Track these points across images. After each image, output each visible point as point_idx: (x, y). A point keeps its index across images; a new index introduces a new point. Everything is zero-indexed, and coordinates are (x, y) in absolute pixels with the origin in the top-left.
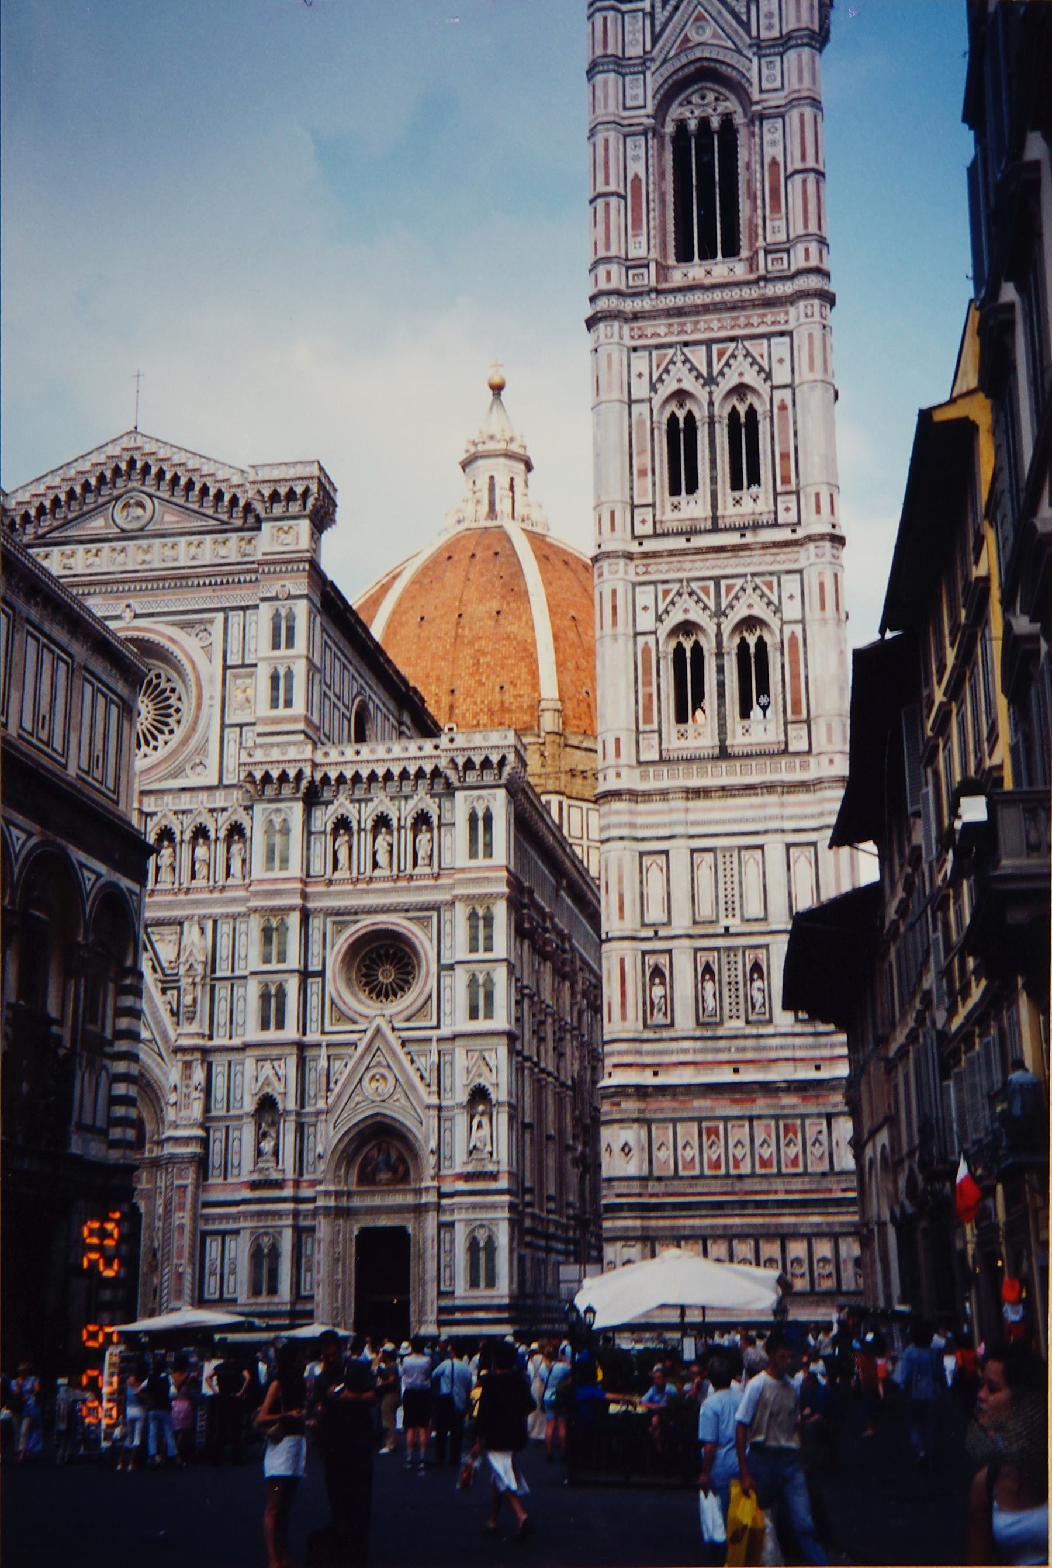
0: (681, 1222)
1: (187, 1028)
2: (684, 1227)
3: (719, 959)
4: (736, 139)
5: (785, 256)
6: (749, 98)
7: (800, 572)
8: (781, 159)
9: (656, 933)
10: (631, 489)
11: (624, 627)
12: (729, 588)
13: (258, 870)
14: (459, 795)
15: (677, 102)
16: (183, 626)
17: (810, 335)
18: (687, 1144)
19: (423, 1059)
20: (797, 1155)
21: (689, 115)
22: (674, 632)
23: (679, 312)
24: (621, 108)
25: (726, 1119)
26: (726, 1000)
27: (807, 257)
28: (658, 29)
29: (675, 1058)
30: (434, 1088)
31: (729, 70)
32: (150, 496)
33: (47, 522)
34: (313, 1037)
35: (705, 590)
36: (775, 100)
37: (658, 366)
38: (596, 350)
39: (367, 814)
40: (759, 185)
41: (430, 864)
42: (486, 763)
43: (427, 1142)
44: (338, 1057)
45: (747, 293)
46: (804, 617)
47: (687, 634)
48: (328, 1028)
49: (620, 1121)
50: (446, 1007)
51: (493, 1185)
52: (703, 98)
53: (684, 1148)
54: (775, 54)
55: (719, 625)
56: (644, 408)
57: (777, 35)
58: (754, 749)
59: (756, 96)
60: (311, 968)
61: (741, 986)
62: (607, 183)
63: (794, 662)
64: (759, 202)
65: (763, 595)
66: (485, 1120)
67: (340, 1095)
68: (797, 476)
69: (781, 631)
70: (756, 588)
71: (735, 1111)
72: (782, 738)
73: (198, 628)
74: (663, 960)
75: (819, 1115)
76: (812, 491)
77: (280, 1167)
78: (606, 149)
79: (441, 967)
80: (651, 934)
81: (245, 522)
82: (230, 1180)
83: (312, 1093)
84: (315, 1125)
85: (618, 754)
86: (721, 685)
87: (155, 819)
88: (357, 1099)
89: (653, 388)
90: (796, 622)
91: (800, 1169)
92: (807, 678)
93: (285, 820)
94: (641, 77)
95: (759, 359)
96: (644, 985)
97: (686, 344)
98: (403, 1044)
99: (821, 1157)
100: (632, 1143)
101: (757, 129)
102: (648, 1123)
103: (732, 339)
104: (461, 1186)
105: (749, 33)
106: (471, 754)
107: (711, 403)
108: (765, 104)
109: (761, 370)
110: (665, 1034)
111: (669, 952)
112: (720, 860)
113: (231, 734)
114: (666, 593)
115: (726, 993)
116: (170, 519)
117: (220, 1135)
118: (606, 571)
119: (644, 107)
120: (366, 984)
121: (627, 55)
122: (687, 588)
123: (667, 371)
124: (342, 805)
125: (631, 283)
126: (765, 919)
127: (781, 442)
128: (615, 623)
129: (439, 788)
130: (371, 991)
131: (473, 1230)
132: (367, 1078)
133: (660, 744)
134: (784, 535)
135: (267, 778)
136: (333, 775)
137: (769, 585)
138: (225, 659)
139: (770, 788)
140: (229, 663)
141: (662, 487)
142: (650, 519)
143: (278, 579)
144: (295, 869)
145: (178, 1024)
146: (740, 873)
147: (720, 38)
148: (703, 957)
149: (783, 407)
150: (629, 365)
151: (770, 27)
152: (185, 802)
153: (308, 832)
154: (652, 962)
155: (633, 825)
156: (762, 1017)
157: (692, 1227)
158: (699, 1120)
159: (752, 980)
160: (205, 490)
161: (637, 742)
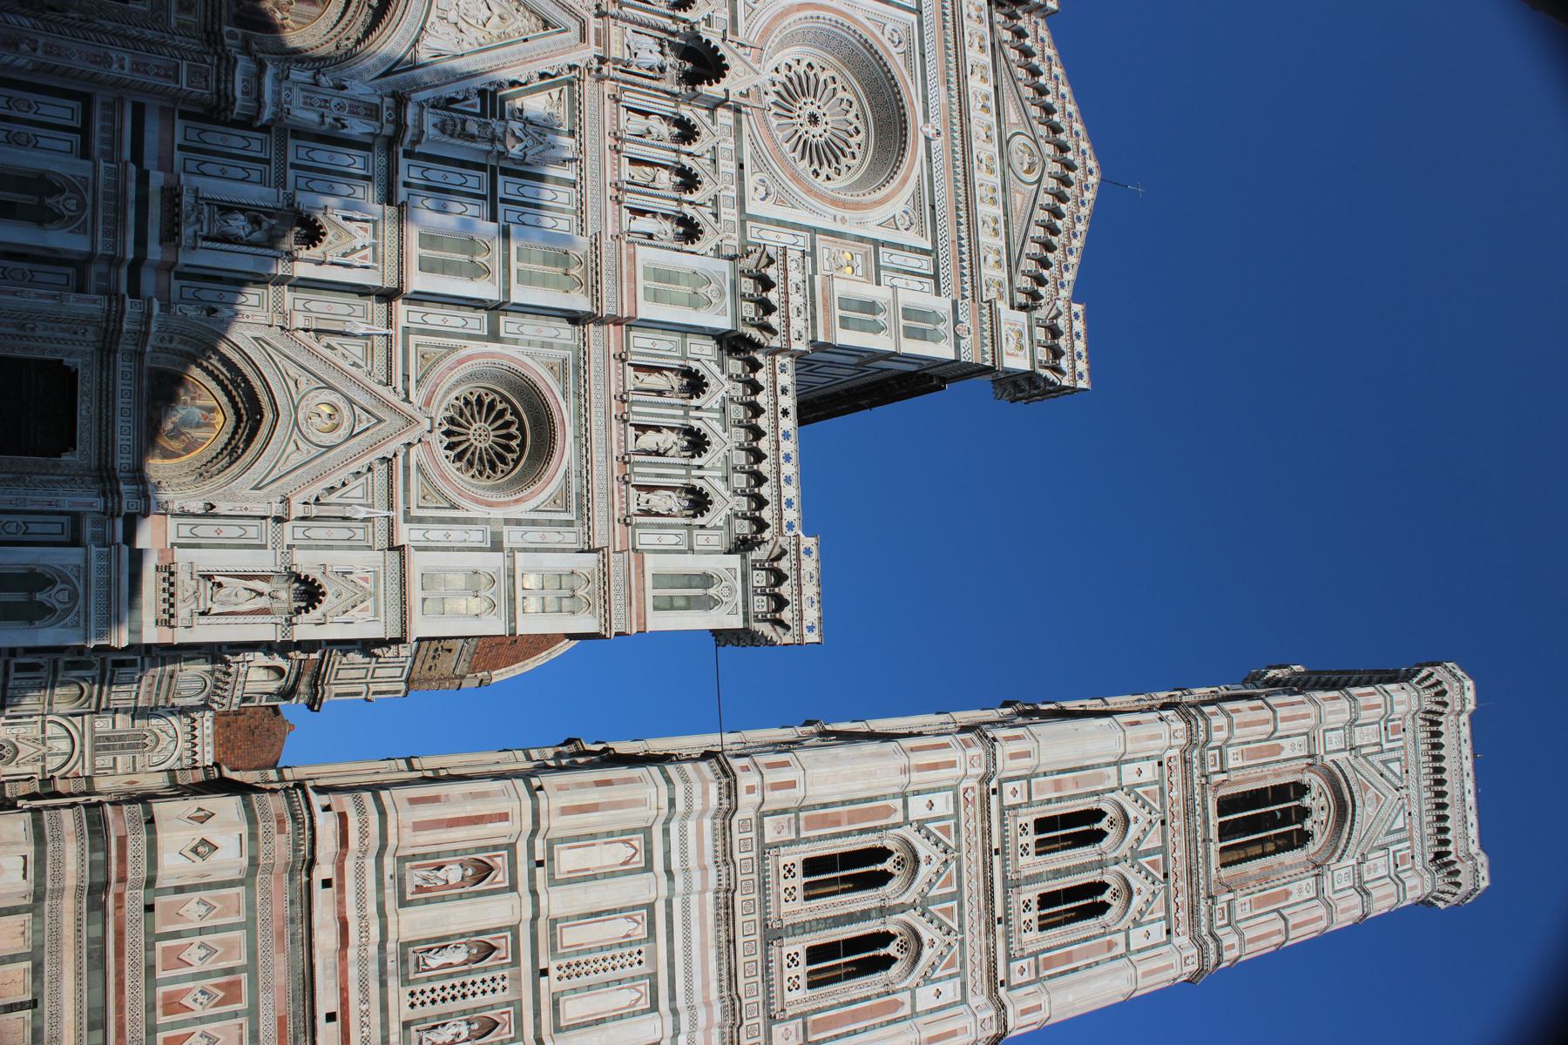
1: (430, 119)
3: (502, 967)
7: (964, 1001)
8: (1292, 900)
9: (540, 864)
12: (949, 912)
13: (646, 255)
14: (735, 560)
15: (1322, 783)
16: (917, 196)
19: (358, 492)
21: (1313, 795)
25: (253, 1013)
29: (352, 914)
30: (315, 511)
32: (1039, 181)
33: (1014, 55)
37: (1146, 793)
42: (781, 603)
43: (225, 498)
44: (370, 352)
48: (413, 339)
49: (253, 836)
50: (437, 534)
53: (202, 946)
55: (913, 906)
61: (460, 1004)
63: (872, 1012)
67: (310, 351)
68: (1050, 977)
69: (903, 990)
72: (789, 1013)
73: (915, 216)
74: (501, 878)
76: (1043, 1000)
77: (200, 243)
81: (1019, 290)
82: (178, 155)
87: (708, 121)
88: (302, 380)
90: (913, 1006)
92: (855, 1032)
97: (1163, 823)
98: (384, 459)
100: (215, 857)
102: (248, 879)
103: (1166, 876)
109: (1141, 913)
111: (513, 887)
113: (803, 240)
114: (945, 830)
116: (1019, 201)
117: (255, 149)
118: (971, 752)
119: (1326, 753)
128: (921, 768)
131: (66, 580)
135: (767, 284)
137: (950, 965)
138: (884, 244)
140: (881, 249)
142: (1018, 800)
144: (646, 311)
145: (433, 107)
148: (503, 943)
149: (1111, 945)
150: (1148, 758)
152: (727, 166)
158: (252, 968)
159: (469, 1023)
161: (785, 811)
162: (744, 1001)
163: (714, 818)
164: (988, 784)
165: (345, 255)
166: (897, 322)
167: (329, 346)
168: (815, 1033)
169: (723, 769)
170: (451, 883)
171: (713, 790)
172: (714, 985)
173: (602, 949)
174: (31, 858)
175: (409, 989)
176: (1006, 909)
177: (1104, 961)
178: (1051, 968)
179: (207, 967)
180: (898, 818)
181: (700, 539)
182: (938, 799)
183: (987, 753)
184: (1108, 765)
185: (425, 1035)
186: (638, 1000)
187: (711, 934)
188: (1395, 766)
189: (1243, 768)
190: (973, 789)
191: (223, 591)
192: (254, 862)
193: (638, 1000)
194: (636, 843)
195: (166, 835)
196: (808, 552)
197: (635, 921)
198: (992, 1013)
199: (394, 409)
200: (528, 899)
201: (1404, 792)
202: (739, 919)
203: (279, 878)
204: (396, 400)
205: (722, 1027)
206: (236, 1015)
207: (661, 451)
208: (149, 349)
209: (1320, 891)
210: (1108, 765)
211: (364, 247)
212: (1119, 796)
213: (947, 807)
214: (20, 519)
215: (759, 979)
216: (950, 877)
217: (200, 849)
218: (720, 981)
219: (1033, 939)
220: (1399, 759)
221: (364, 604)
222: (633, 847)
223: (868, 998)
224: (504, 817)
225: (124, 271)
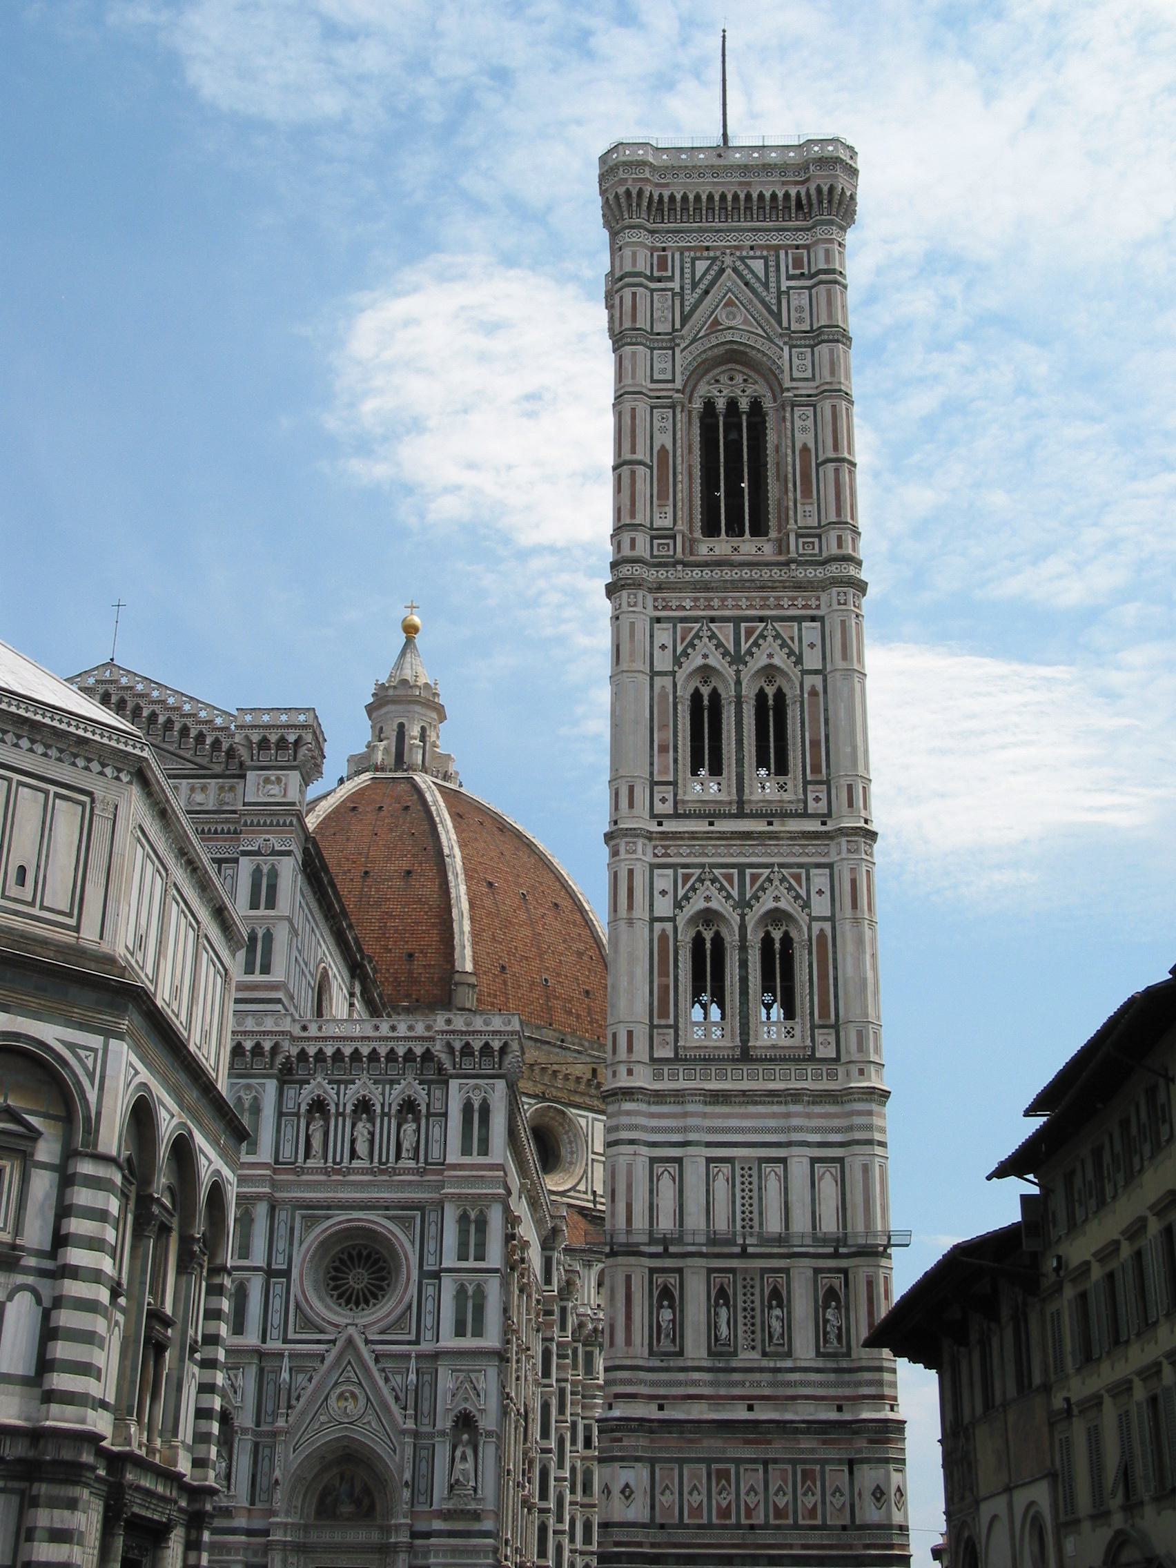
3: (735, 1282)
4: (765, 422)
5: (816, 540)
6: (780, 385)
7: (830, 866)
8: (811, 445)
9: (666, 1249)
10: (652, 764)
11: (641, 912)
12: (755, 878)
14: (454, 1084)
15: (706, 379)
17: (843, 622)
19: (398, 1378)
20: (815, 1504)
22: (693, 920)
23: (706, 587)
24: (648, 380)
25: (738, 1462)
27: (840, 546)
28: (687, 309)
30: (411, 1412)
31: (759, 355)
34: (274, 1345)
35: (729, 878)
36: (806, 388)
37: (683, 640)
38: (617, 618)
39: (351, 1094)
40: (790, 468)
41: (416, 1158)
43: (403, 1471)
45: (776, 573)
46: (833, 915)
47: (707, 923)
48: (291, 1336)
49: (622, 1459)
50: (428, 1320)
51: (477, 1526)
52: (731, 379)
53: (690, 1493)
54: (806, 346)
55: (743, 916)
56: (668, 681)
57: (808, 328)
58: (778, 1053)
59: (787, 384)
62: (633, 451)
64: (790, 485)
66: (469, 1452)
67: (303, 1413)
68: (828, 766)
69: (810, 928)
70: (783, 880)
71: (748, 1453)
72: (808, 1042)
74: (673, 1279)
75: (840, 1462)
76: (844, 782)
78: (633, 418)
79: (423, 1274)
80: (660, 1249)
83: (270, 1410)
84: (272, 1447)
85: (630, 1049)
86: (744, 981)
89: (677, 661)
90: (824, 919)
91: (819, 1522)
92: (836, 979)
93: (255, 1098)
94: (670, 352)
95: (789, 642)
96: (651, 1306)
97: (713, 620)
98: (377, 1360)
99: (841, 1510)
100: (632, 1484)
101: (788, 415)
102: (652, 1462)
103: (761, 619)
104: (438, 1525)
105: (780, 324)
106: (469, 1038)
107: (738, 683)
108: (796, 392)
111: (680, 1271)
112: (738, 1172)
114: (686, 877)
118: (622, 849)
119: (673, 381)
120: (335, 1288)
121: (655, 331)
122: (706, 874)
123: (692, 645)
124: (319, 1086)
125: (655, 553)
127: (811, 728)
128: (630, 907)
132: (334, 1396)
133: (676, 1041)
134: (813, 826)
136: (312, 1051)
139: (795, 1096)
142: (670, 797)
143: (262, 832)
144: (265, 1154)
146: (760, 1188)
147: (751, 325)
148: (717, 1279)
149: (814, 693)
150: (652, 636)
151: (800, 320)
153: (280, 1114)
154: (660, 1281)
155: (644, 1129)
156: (780, 1349)
158: (708, 1461)
159: (770, 1307)
160: (185, 731)
163: (649, 1103)
164: (651, 833)
165: (235, 1392)
167: (298, 1399)
168: (829, 1016)
170: (671, 1317)
171: (627, 1106)
172: (776, 1109)
173: (734, 1202)
177: (826, 703)
178: (820, 766)
179: (704, 1492)
181: (437, 1107)
183: (626, 835)
184: (652, 686)
186: (776, 1174)
188: (701, 266)
189: (675, 506)
190: (655, 847)
191: (461, 1479)
192: (638, 1459)
194: (661, 1170)
195: (615, 1516)
196: (449, 1022)
197: (717, 1173)
200: (690, 1261)
201: (728, 260)
203: (652, 1441)
204: (335, 1351)
205: (808, 1102)
206: (738, 1473)
208: (302, 1522)
209: (811, 402)
210: (652, 686)
211: (230, 1379)
212: (681, 675)
213: (668, 876)
215: (777, 1068)
217: (627, 1494)
220: (693, 260)
221: (474, 1380)
222: (663, 1173)
224: (628, 1279)
225: (253, 1540)
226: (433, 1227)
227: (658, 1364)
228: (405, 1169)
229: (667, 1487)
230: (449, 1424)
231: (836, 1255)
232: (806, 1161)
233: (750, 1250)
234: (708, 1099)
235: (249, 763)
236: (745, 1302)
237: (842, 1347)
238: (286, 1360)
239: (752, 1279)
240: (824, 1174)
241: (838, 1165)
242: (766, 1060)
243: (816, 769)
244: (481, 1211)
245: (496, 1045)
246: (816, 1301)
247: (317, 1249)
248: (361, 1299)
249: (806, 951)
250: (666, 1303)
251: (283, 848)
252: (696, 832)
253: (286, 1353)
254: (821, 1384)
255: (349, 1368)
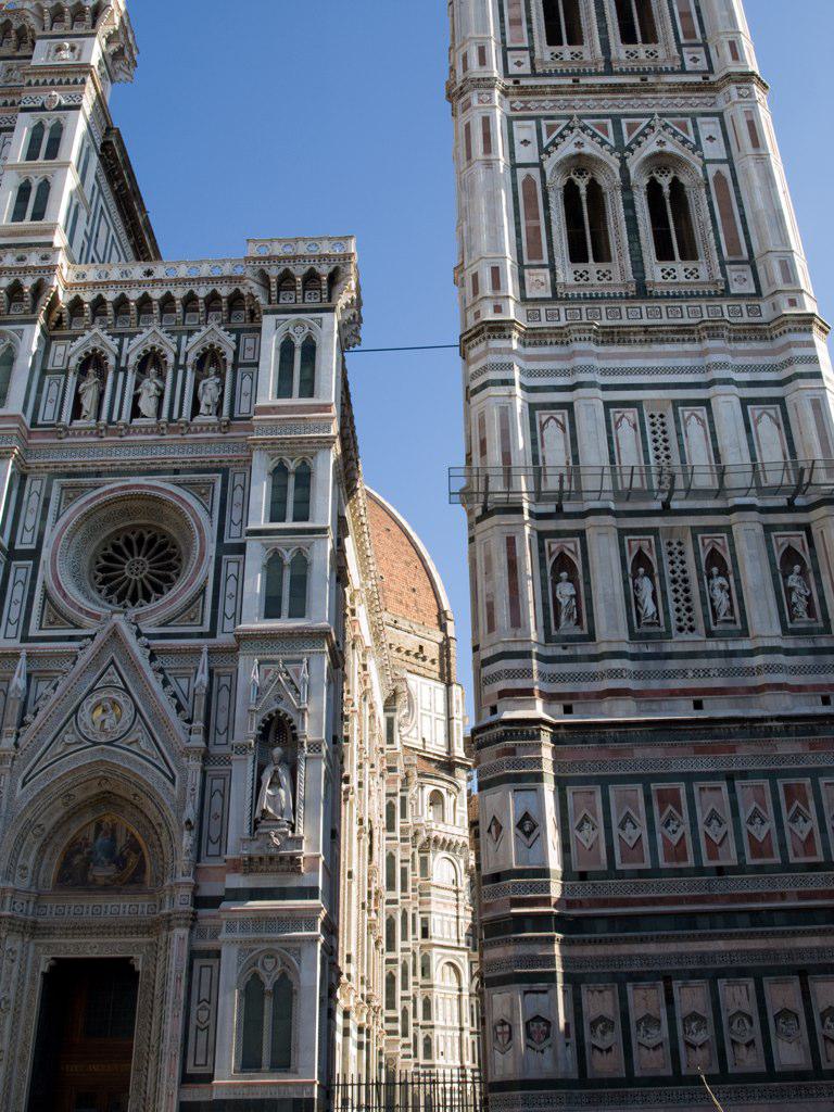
0: (625, 949)
2: (630, 957)
3: (658, 544)
9: (559, 508)
12: (631, 128)
14: (268, 322)
18: (628, 817)
19: (184, 683)
20: (811, 835)
22: (560, 165)
25: (689, 778)
26: (672, 606)
30: (199, 724)
39: (134, 349)
41: (219, 412)
42: (311, 277)
47: (580, 172)
48: (33, 632)
50: (229, 607)
53: (622, 826)
55: (623, 160)
60: (18, 547)
65: (675, 134)
68: (703, 31)
69: (704, 170)
71: (703, 764)
72: (719, 276)
74: (571, 546)
79: (223, 549)
88: (68, 738)
90: (721, 161)
91: (820, 858)
92: (743, 217)
96: (543, 579)
98: (152, 658)
104: (237, 881)
110: (580, 650)
111: (581, 534)
112: (647, 421)
114: (551, 129)
115: (671, 596)
118: (475, 102)
126: (720, 493)
129: (240, 320)
130: (111, 591)
132: (86, 707)
137: (684, 127)
139: (713, 331)
141: (540, 36)
142: (527, 61)
148: (634, 543)
154: (554, 547)
157: (644, 958)
158: (645, 780)
159: (710, 577)
162: (706, 318)
166: (38, 166)
167: (35, 714)
168: (741, 254)
169: (476, 335)
170: (574, 592)
172: (688, 347)
173: (646, 451)
174: (526, 986)
175: (674, 631)
176: (632, 73)
178: (694, 32)
179: (643, 822)
180: (535, 173)
181: (249, 356)
182: (519, 135)
183: (477, 87)
185: (721, 617)
186: (698, 418)
187: (638, 349)
190: (512, 103)
193: (696, 416)
194: (544, 418)
198: (732, 88)
199: (102, 649)
200: (591, 520)
202: (625, 322)
204: (92, 648)
206: (690, 796)
207: (159, 394)
213: (530, 127)
214: (194, 1008)
215: (684, 305)
216: (598, 126)
217: (527, 829)
218: (684, 340)
219: (665, 50)
222: (548, 420)
223: (710, 204)
226: (239, 491)
227: (559, 651)
228: (202, 425)
229: (585, 818)
230: (253, 731)
231: (791, 508)
232: (736, 402)
233: (675, 505)
234: (600, 338)
235: (39, 32)
236: (673, 572)
237: (817, 621)
238: (22, 662)
239: (680, 544)
240: (760, 416)
241: (778, 406)
242: (668, 296)
243: (689, 34)
244: (304, 463)
245: (324, 270)
246: (772, 564)
247: (78, 525)
248: (140, 593)
249: (704, 190)
250: (564, 575)
251: (72, 103)
252: (560, 86)
253: (23, 653)
254: (794, 670)
255: (112, 667)
